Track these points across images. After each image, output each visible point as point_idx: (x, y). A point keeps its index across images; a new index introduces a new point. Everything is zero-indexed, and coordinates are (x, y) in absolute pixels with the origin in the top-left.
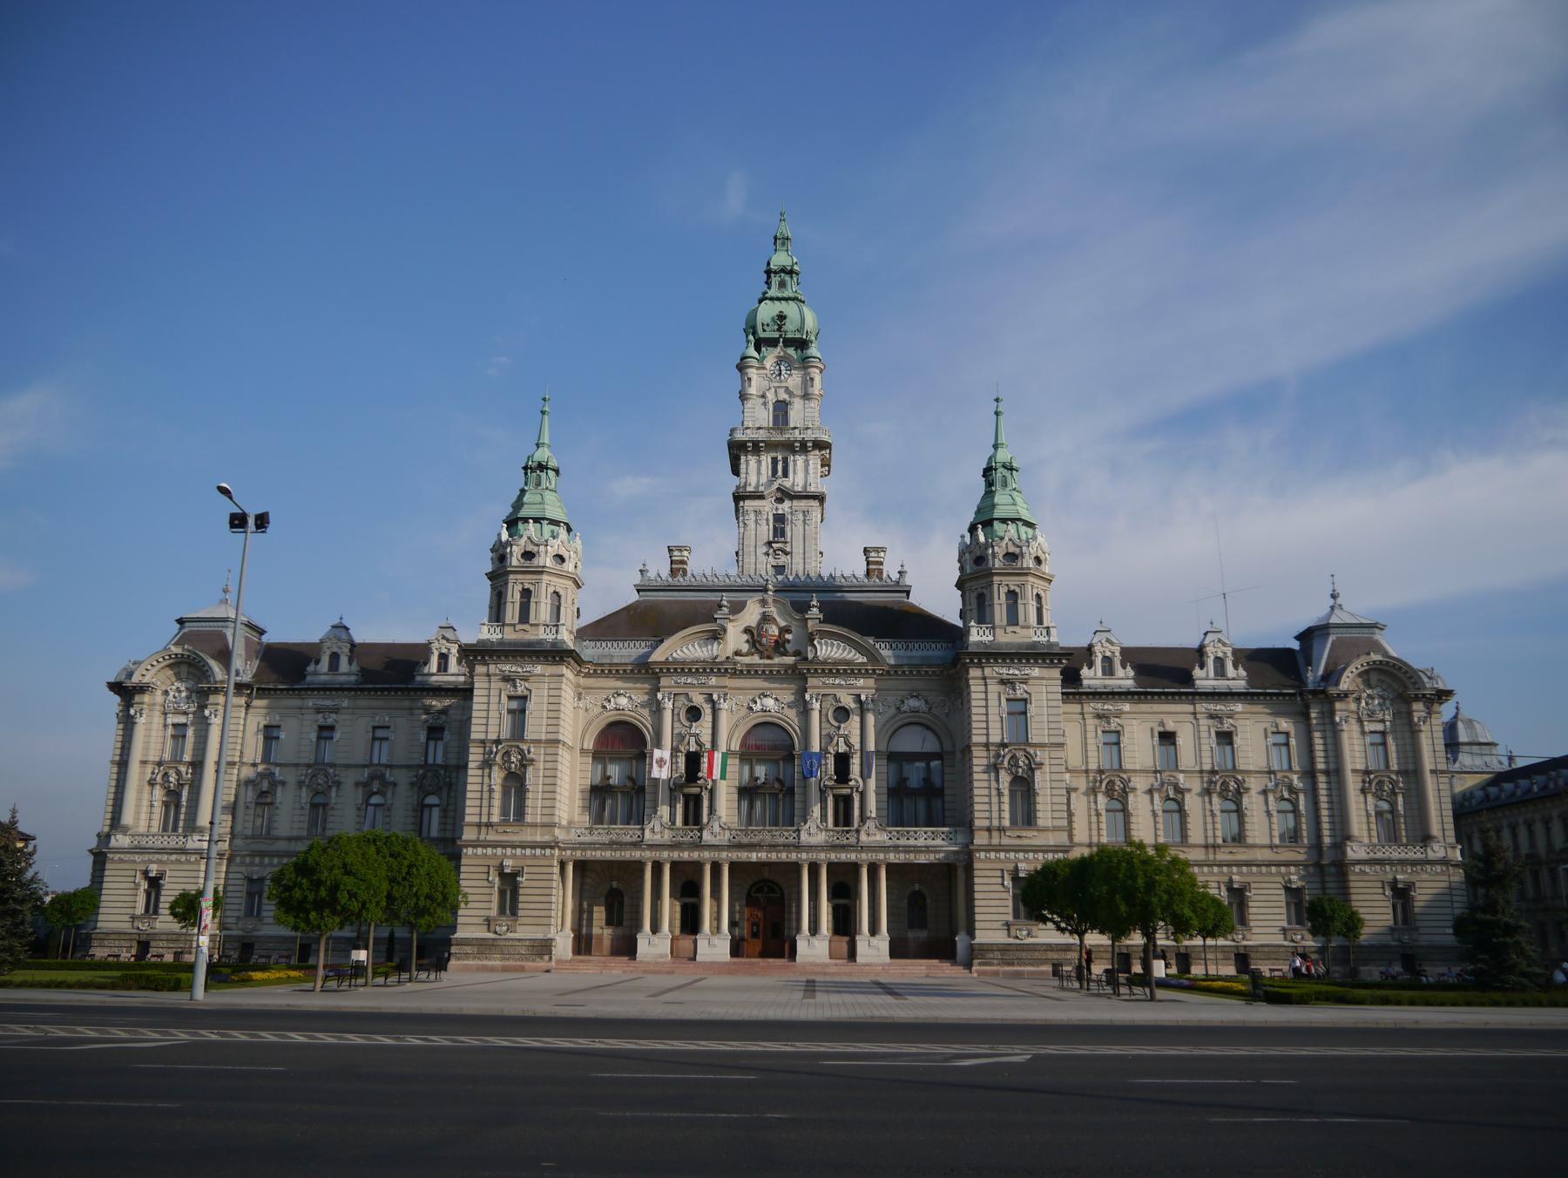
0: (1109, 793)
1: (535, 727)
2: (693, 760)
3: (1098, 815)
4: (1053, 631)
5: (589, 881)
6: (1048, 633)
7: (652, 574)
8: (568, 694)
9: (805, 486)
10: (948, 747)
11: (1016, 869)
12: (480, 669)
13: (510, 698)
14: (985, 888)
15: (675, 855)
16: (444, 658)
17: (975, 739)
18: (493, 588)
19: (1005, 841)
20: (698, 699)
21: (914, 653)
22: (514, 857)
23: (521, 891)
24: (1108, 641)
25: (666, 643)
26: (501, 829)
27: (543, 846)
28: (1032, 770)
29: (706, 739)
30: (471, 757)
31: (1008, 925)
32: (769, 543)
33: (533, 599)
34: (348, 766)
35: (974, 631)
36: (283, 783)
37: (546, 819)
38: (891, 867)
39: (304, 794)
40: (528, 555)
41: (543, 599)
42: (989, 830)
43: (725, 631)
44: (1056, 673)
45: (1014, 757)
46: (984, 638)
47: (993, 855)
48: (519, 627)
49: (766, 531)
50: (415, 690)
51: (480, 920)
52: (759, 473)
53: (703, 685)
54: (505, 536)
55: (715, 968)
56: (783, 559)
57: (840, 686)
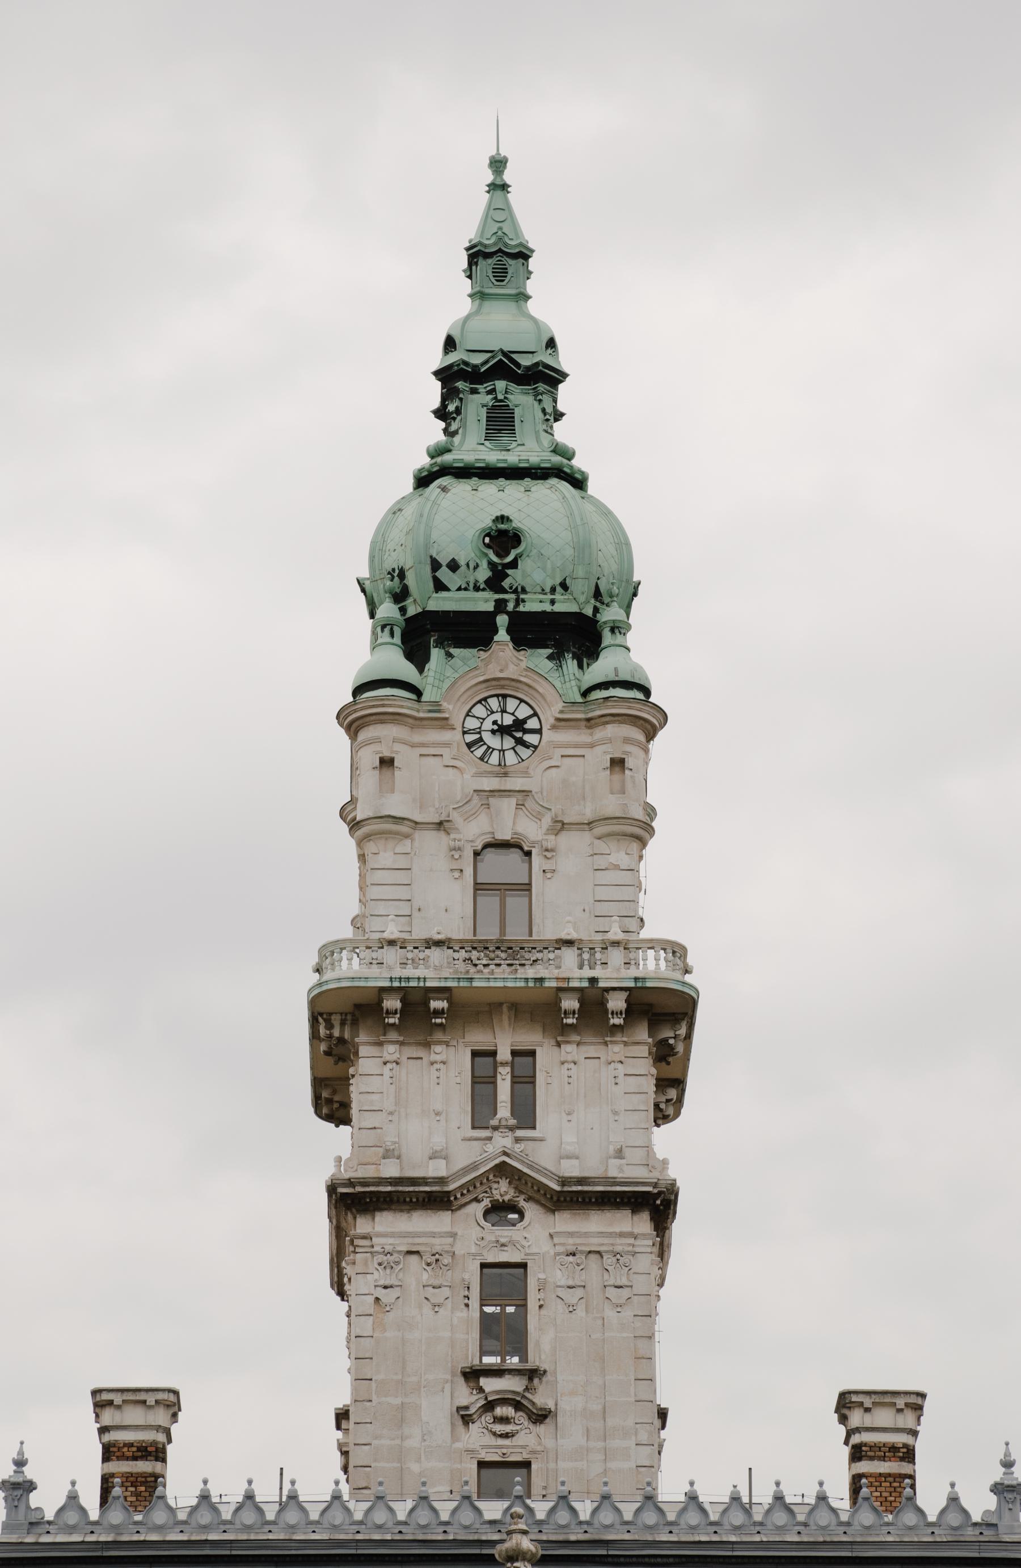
49: (453, 1330)
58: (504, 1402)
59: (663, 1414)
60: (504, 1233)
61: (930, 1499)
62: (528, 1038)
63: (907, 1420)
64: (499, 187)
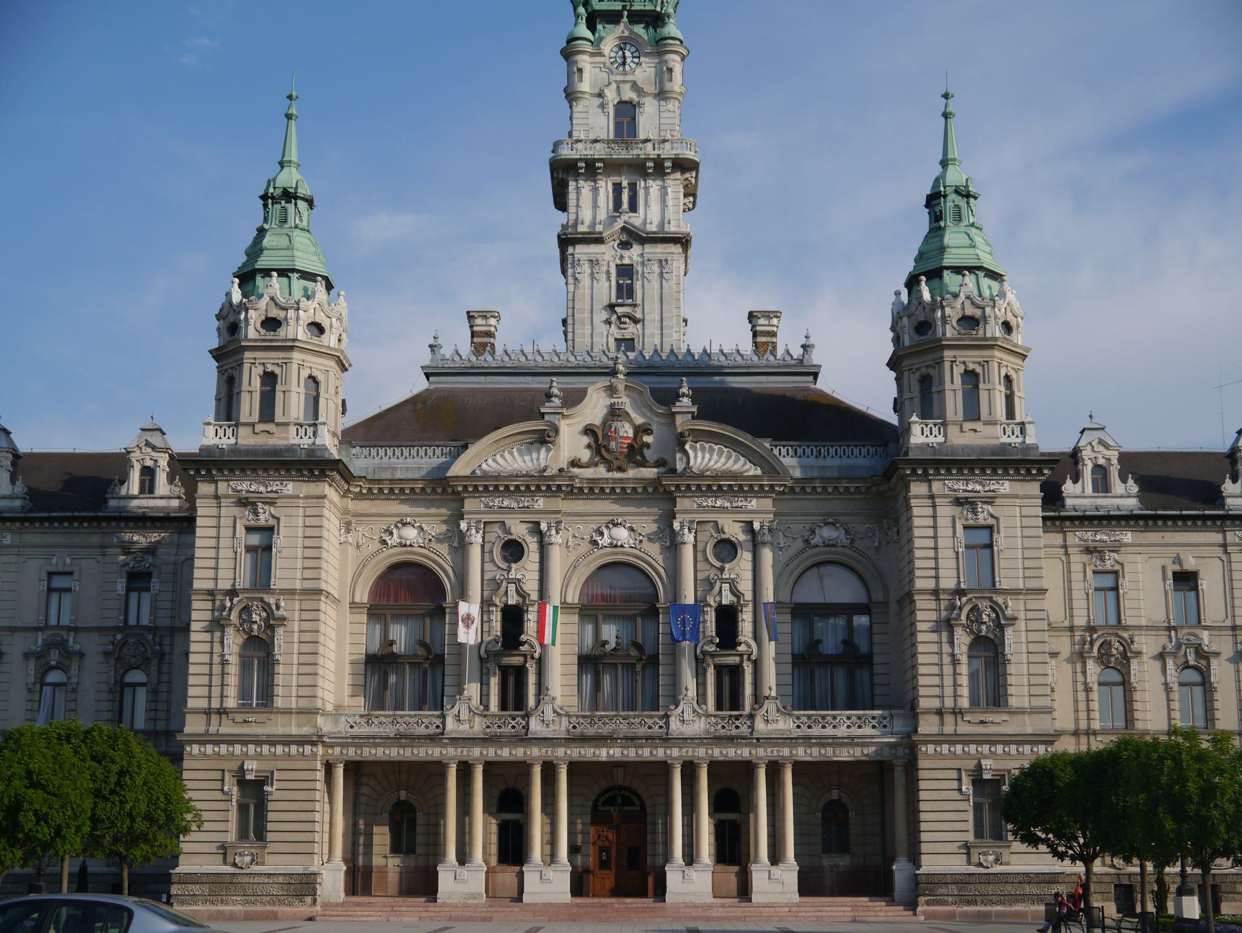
0: (1104, 659)
1: (287, 570)
2: (513, 618)
3: (1088, 690)
4: (1030, 429)
5: (365, 790)
6: (1023, 432)
7: (447, 351)
8: (331, 523)
9: (662, 224)
10: (878, 596)
11: (979, 768)
12: (204, 488)
13: (249, 529)
14: (935, 795)
15: (491, 753)
16: (148, 473)
17: (920, 584)
18: (221, 371)
19: (963, 729)
20: (519, 530)
21: (829, 462)
22: (259, 757)
23: (271, 806)
24: (1101, 442)
25: (473, 450)
26: (239, 718)
27: (302, 741)
28: (1001, 628)
29: (531, 587)
30: (195, 615)
31: (967, 847)
32: (611, 307)
33: (279, 388)
34: (13, 630)
35: (916, 429)
37: (304, 703)
38: (801, 769)
40: (271, 324)
41: (294, 388)
42: (940, 712)
43: (557, 431)
44: (1034, 489)
45: (975, 609)
46: (931, 440)
47: (945, 748)
48: (259, 428)
49: (606, 290)
50: (109, 519)
51: (212, 848)
52: (595, 206)
53: (526, 510)
54: (237, 296)
55: (551, 912)
56: (631, 330)
57: (723, 510)
58: (625, 316)
59: (685, 321)
60: (626, 253)
61: (780, 352)
62: (634, 178)
63: (775, 321)
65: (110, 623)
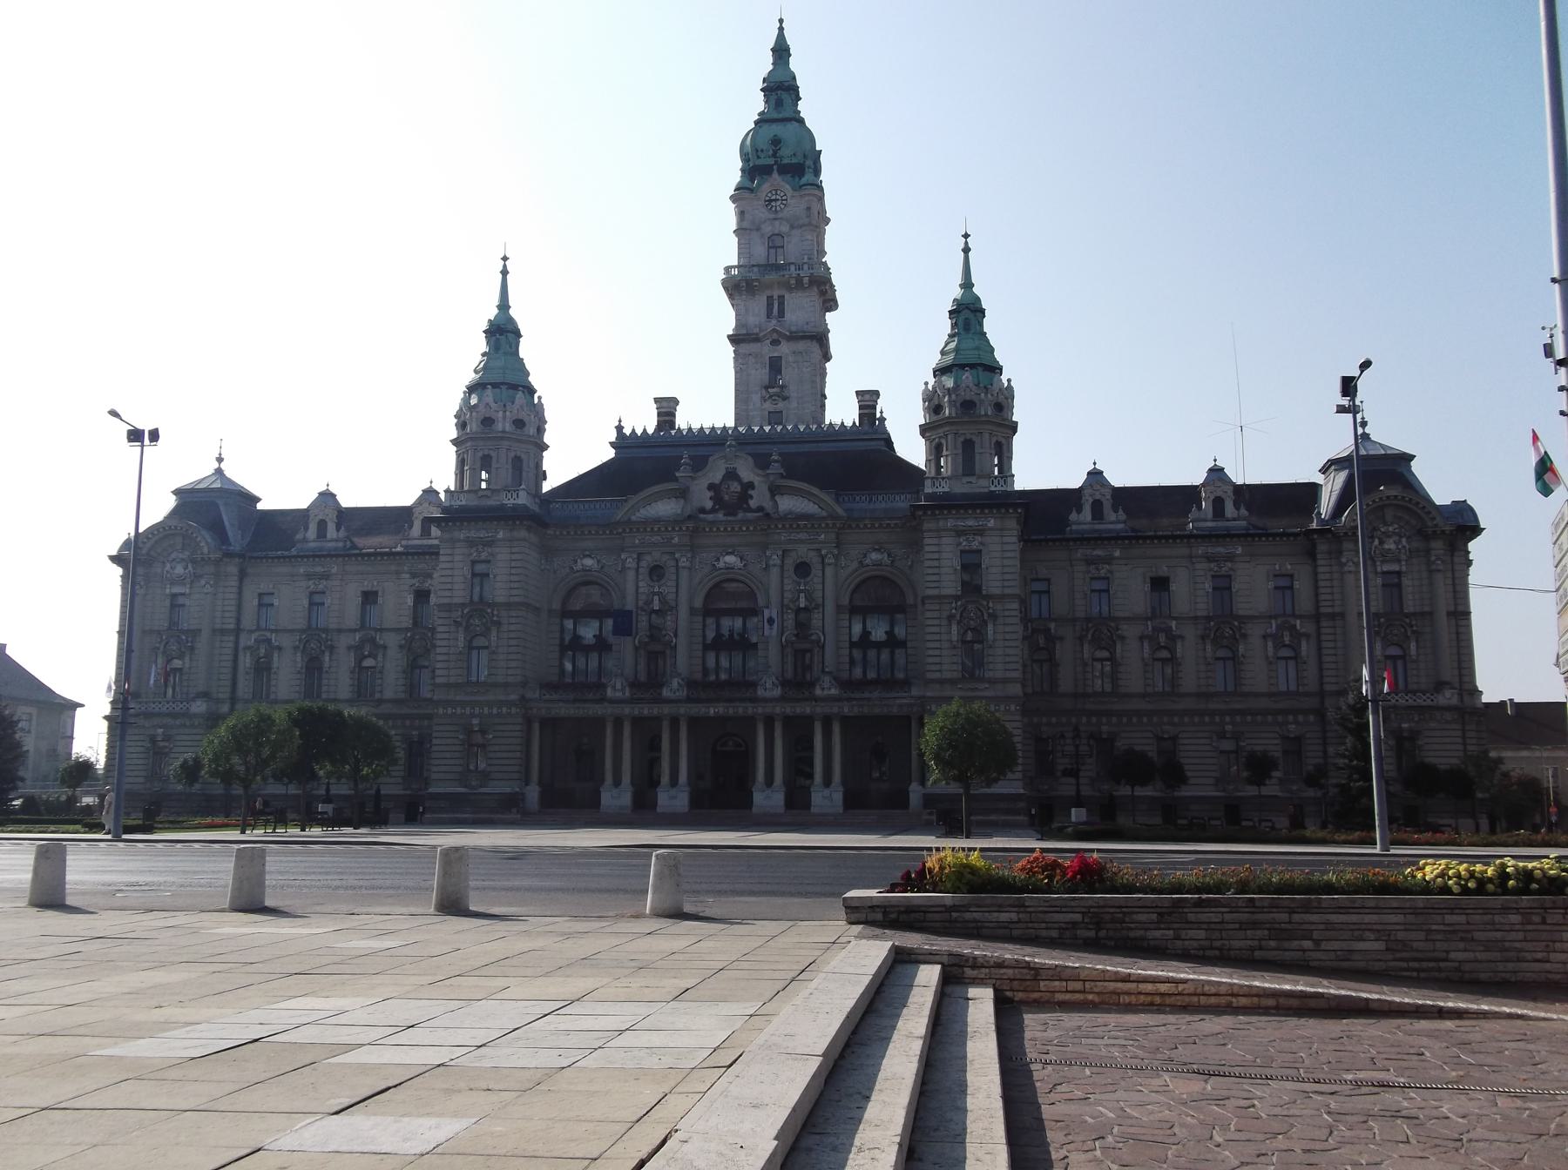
3: (1086, 665)
7: (627, 431)
25: (634, 499)
32: (766, 388)
34: (340, 631)
36: (280, 648)
38: (846, 721)
39: (299, 659)
44: (1012, 524)
49: (762, 374)
56: (781, 405)
64: (781, 29)
65: (404, 625)
